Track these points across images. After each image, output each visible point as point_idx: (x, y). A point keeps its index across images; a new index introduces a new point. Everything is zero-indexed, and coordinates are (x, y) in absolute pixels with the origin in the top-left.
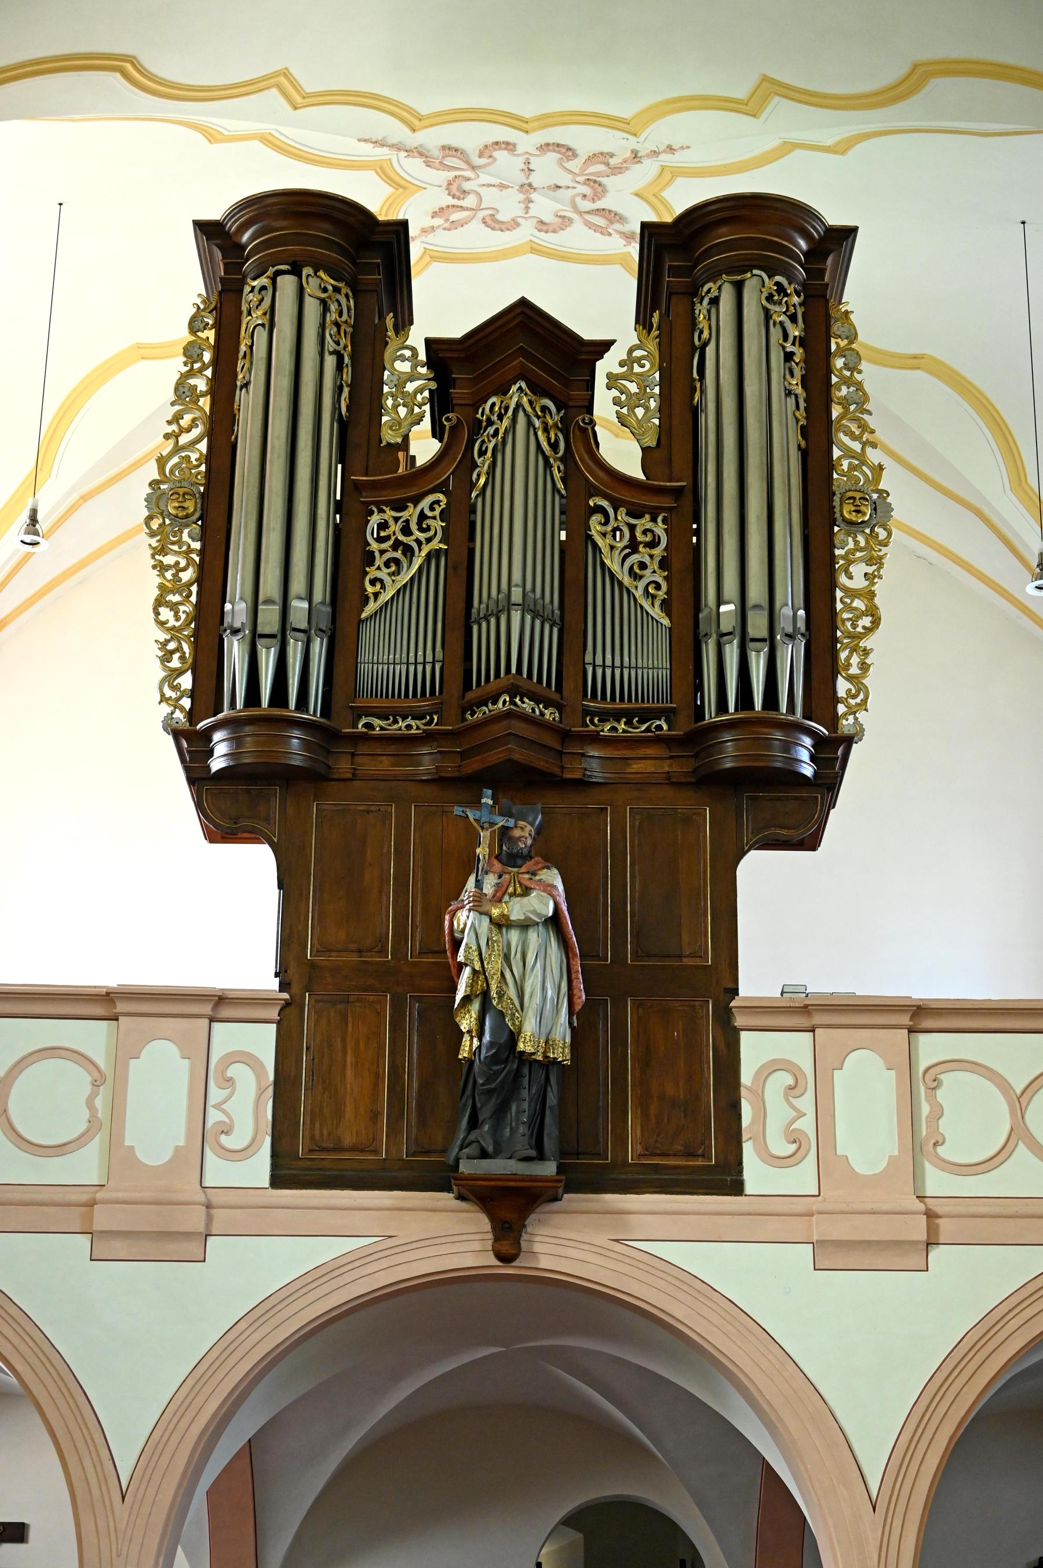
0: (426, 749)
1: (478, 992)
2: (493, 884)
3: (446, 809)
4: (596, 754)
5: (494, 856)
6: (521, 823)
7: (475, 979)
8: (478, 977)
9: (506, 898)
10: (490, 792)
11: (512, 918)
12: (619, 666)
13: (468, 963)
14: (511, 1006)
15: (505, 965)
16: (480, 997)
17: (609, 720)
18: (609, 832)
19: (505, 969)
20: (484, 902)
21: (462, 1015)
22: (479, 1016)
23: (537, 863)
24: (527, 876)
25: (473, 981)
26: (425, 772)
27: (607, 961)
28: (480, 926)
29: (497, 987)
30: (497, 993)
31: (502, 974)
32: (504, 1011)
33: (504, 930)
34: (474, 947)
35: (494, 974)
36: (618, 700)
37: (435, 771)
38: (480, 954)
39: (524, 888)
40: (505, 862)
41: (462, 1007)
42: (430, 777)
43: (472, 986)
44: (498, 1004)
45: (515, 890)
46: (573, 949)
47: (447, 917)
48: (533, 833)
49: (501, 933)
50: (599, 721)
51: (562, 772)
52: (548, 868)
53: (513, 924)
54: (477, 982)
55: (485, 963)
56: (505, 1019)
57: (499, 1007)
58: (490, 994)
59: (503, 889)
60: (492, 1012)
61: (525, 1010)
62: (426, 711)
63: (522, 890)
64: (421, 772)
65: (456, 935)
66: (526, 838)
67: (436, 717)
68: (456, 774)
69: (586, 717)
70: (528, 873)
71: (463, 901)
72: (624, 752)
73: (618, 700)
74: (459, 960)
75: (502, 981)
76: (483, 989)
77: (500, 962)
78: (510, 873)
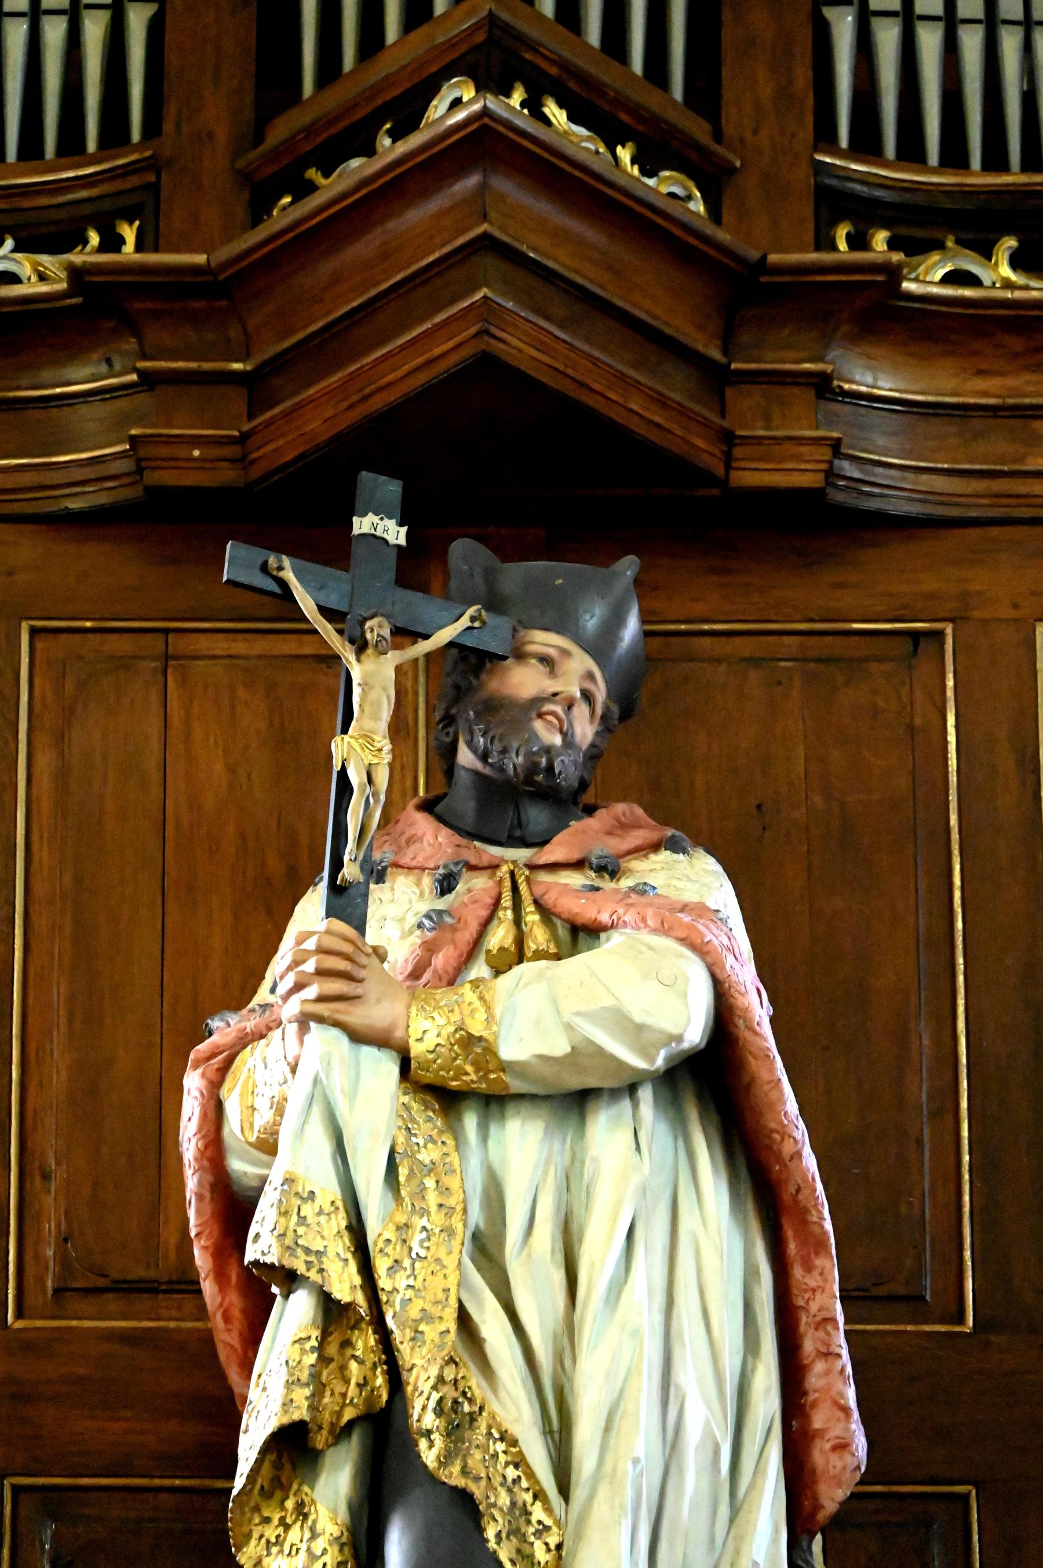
0: (86, 371)
1: (349, 1414)
2: (412, 920)
3: (179, 644)
4: (886, 386)
5: (415, 801)
6: (543, 640)
7: (332, 1350)
8: (347, 1344)
9: (480, 969)
10: (392, 488)
11: (508, 1052)
12: (980, 15)
13: (301, 1268)
14: (511, 1473)
15: (477, 1280)
16: (355, 1438)
17: (939, 246)
18: (952, 738)
19: (480, 1304)
20: (371, 988)
21: (271, 1532)
22: (353, 1529)
23: (624, 826)
24: (575, 879)
25: (324, 1360)
26: (78, 474)
27: (961, 1319)
28: (352, 1095)
29: (441, 1380)
30: (439, 1411)
31: (464, 1319)
32: (477, 1491)
33: (470, 1121)
34: (329, 1190)
35: (426, 1317)
36: (976, 162)
37: (125, 466)
38: (357, 1231)
39: (563, 932)
40: (469, 821)
41: (266, 1494)
42: (103, 499)
43: (319, 1387)
44: (446, 1459)
45: (520, 941)
46: (803, 1216)
47: (193, 1082)
48: (601, 693)
49: (454, 1128)
50: (893, 244)
51: (728, 460)
52: (674, 846)
53: (516, 1085)
54: (343, 1368)
55: (381, 1265)
56: (481, 1530)
57: (453, 1476)
58: (407, 1416)
59: (467, 935)
60: (418, 1495)
61: (579, 1494)
62: (87, 210)
63: (554, 936)
64: (58, 477)
65: (239, 1166)
66: (570, 706)
67: (129, 233)
68: (227, 475)
69: (834, 224)
70: (579, 865)
71: (265, 1007)
72: (1011, 382)
73: (976, 162)
74: (251, 1253)
75: (463, 1355)
76: (371, 1398)
77: (451, 1262)
78: (494, 867)
